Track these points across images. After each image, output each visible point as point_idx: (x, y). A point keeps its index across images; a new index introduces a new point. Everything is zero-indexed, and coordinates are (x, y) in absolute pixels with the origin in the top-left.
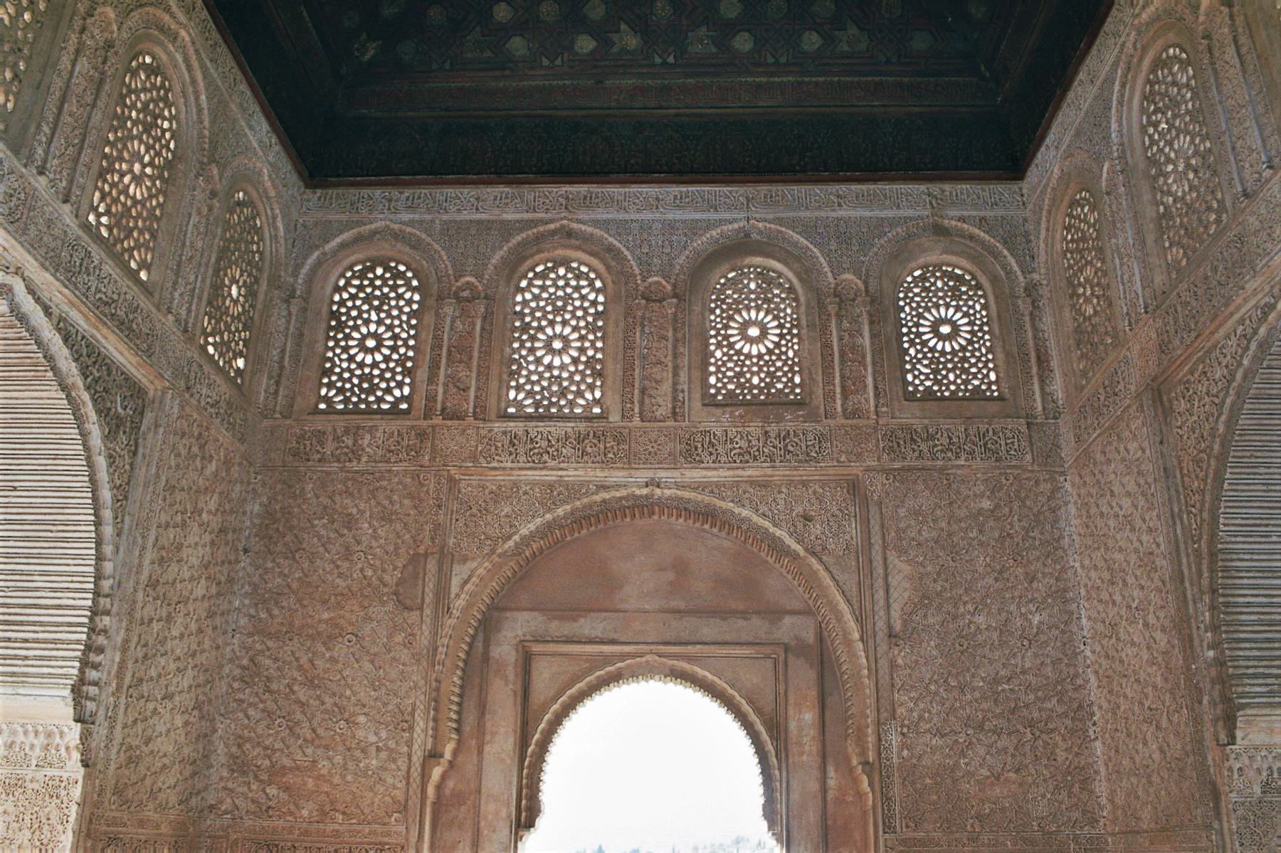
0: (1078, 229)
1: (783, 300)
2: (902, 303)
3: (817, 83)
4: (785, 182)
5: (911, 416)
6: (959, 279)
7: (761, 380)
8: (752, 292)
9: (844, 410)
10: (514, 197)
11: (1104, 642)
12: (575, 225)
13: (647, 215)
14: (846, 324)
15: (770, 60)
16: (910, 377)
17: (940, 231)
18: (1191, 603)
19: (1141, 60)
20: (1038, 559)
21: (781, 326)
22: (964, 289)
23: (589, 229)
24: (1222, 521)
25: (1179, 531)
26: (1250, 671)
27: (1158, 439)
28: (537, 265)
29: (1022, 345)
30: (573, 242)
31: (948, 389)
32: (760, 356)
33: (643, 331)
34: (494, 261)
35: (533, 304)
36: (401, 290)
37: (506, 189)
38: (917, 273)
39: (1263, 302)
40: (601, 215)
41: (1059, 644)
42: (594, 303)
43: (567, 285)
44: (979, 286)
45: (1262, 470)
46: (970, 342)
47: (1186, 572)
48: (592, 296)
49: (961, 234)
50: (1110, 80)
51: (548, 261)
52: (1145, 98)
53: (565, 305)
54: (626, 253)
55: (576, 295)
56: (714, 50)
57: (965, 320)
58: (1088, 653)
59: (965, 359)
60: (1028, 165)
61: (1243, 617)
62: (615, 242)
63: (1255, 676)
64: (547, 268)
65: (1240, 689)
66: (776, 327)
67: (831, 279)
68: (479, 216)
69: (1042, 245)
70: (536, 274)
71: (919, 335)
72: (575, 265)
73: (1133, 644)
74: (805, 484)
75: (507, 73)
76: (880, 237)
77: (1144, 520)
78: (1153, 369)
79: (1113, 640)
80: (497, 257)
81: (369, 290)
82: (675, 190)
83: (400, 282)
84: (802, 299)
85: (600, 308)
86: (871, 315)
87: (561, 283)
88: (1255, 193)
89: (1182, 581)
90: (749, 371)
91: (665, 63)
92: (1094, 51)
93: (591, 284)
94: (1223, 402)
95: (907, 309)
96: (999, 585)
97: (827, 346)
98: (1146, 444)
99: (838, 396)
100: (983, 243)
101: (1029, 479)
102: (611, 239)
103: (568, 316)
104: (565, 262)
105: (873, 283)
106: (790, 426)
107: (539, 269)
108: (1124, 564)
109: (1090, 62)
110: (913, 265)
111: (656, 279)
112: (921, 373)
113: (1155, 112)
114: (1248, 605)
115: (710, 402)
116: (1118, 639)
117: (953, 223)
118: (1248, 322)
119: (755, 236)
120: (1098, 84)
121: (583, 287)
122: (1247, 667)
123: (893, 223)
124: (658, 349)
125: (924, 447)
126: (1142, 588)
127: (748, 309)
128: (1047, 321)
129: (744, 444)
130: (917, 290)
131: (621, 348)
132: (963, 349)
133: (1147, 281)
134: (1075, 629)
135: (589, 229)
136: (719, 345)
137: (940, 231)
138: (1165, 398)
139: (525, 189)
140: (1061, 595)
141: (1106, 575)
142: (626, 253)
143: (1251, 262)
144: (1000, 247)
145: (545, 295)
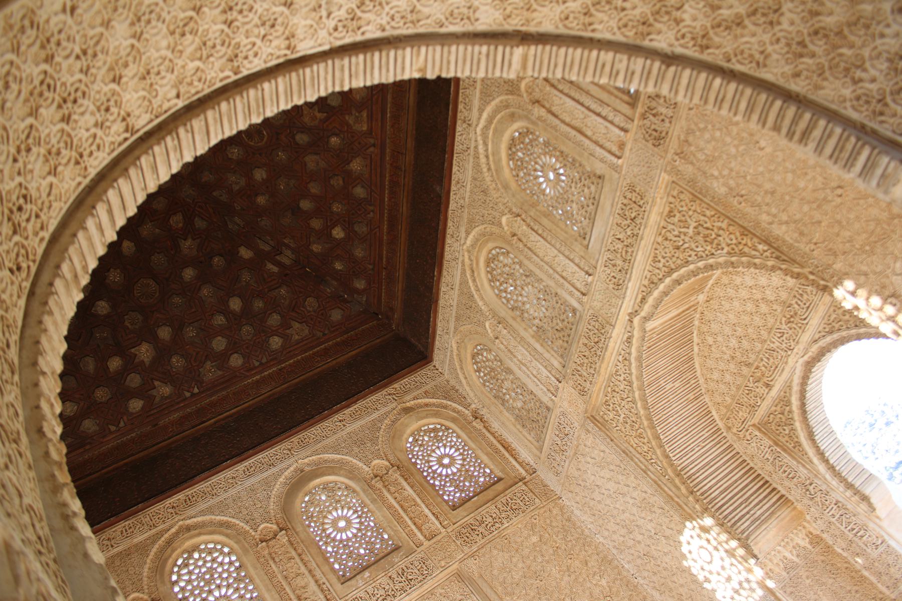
0: (485, 367)
1: (346, 496)
2: (413, 460)
3: (290, 365)
4: (305, 429)
5: (464, 517)
6: (434, 430)
7: (365, 549)
8: (325, 501)
9: (425, 537)
10: (135, 526)
11: (648, 567)
12: (189, 522)
13: (232, 492)
14: (392, 489)
15: (257, 364)
16: (446, 498)
17: (407, 410)
18: (685, 507)
19: (477, 264)
20: (581, 551)
21: (356, 512)
22: (441, 434)
23: (200, 519)
24: (671, 455)
25: (653, 476)
26: (737, 518)
27: (608, 440)
28: (177, 560)
29: (491, 445)
30: (193, 532)
31: (470, 491)
32: (355, 536)
33: (275, 562)
34: (145, 574)
35: (189, 587)
36: (220, 560)
37: (127, 523)
38: (411, 440)
39: (625, 338)
40: (202, 506)
41: (624, 588)
42: (231, 563)
43: (205, 562)
44: (447, 429)
45: (671, 419)
46: (464, 460)
47: (671, 493)
48: (227, 560)
49: (420, 406)
50: (463, 283)
51: (183, 553)
52: (490, 281)
53: (212, 576)
54: (233, 520)
55: (215, 566)
56: (220, 373)
57: (453, 450)
58: (642, 582)
59: (467, 471)
60: (433, 351)
61: (713, 495)
62: (222, 518)
63: (740, 519)
64: (185, 559)
65: (740, 530)
66: (354, 513)
67: (367, 469)
68: (116, 550)
69: (468, 388)
70: (179, 567)
71: (434, 472)
72: (203, 547)
73: (666, 554)
74: (432, 593)
75: (88, 447)
76: (379, 431)
77: (628, 486)
78: (582, 407)
79: (653, 562)
80: (146, 570)
81: (197, 571)
82: (241, 467)
83: (215, 555)
84: (358, 489)
85: (237, 564)
86: (403, 476)
87: (200, 563)
88: (589, 291)
89: (673, 499)
90: (355, 548)
91: (193, 395)
92: (445, 273)
93: (222, 552)
94: (634, 397)
95: (418, 462)
96: (573, 577)
97: (390, 507)
98: (603, 448)
99: (416, 531)
100: (434, 405)
101: (545, 512)
102: (218, 518)
103: (218, 582)
104: (196, 548)
105: (391, 457)
106: (402, 564)
107: (180, 562)
108: (632, 517)
109: (446, 278)
110: (405, 436)
111: (262, 526)
112: (450, 492)
113: (501, 284)
114: (710, 488)
115: (345, 580)
116: (655, 559)
117: (412, 402)
118: (623, 352)
119: (307, 469)
120: (457, 287)
121: (217, 557)
122: (734, 517)
123: (381, 420)
124: (292, 567)
125: (481, 529)
126: (651, 520)
127: (330, 512)
128: (495, 426)
129: (382, 592)
130: (416, 449)
131: (268, 582)
132: (463, 465)
133: (548, 366)
134: (625, 573)
135: (200, 519)
136: (326, 543)
137: (407, 410)
138: (597, 418)
139: (141, 516)
140: (606, 561)
141: (623, 531)
142: (233, 520)
143: (608, 323)
144: (445, 402)
145: (194, 577)
